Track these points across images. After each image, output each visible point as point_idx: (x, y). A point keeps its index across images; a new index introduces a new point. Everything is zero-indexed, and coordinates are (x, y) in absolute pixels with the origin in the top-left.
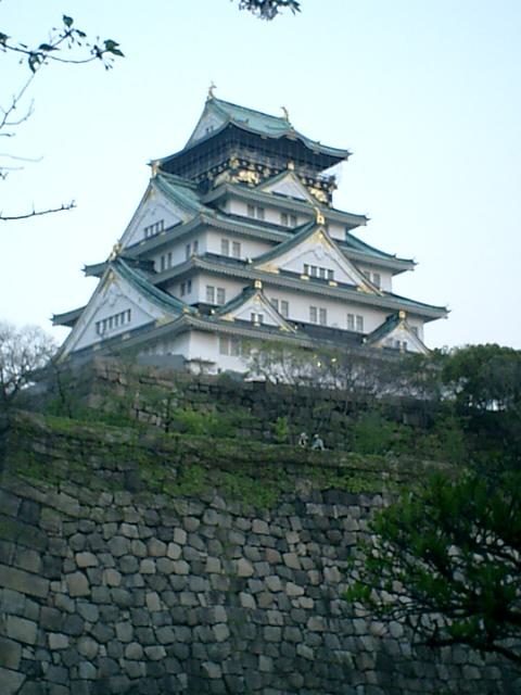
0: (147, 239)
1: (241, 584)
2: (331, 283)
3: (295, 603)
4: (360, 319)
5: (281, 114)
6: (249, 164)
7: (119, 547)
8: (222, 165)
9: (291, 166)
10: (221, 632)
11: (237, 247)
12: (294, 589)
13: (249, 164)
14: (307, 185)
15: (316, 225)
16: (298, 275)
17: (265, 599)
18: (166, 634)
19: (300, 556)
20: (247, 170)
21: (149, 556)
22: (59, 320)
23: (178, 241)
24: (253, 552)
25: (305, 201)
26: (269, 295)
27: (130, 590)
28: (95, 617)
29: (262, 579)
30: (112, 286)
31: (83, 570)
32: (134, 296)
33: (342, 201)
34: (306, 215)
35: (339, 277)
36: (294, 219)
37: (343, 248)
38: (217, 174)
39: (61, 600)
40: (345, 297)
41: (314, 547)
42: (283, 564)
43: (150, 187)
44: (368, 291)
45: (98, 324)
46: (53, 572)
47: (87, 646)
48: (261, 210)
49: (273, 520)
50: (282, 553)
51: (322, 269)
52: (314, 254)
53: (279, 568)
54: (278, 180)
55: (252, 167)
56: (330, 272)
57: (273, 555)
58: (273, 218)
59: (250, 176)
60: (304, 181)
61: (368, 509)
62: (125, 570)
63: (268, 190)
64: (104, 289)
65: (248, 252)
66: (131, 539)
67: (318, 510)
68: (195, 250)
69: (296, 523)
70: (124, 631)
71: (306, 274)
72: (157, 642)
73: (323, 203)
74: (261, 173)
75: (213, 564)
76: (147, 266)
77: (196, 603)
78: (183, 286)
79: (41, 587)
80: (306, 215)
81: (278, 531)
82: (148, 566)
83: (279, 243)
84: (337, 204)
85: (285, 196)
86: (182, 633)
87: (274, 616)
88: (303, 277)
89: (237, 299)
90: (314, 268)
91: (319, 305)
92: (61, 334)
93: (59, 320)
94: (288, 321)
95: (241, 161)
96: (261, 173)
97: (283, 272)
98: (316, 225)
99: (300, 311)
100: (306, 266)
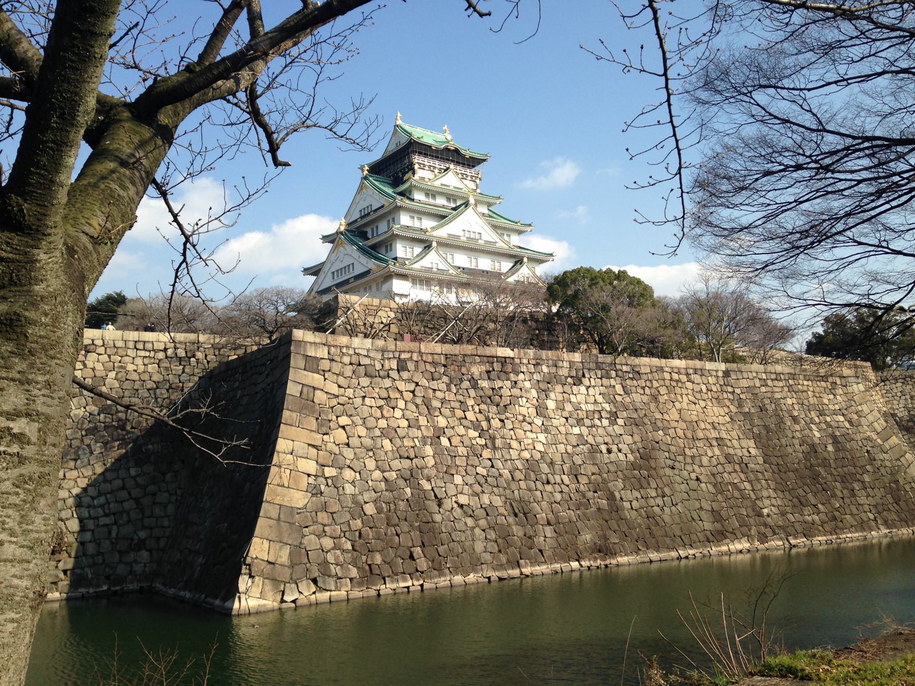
0: (362, 217)
1: (439, 433)
3: (474, 442)
7: (365, 411)
10: (431, 462)
12: (473, 433)
17: (455, 441)
18: (396, 464)
21: (383, 416)
22: (308, 271)
23: (382, 217)
24: (447, 412)
28: (352, 456)
31: (343, 427)
34: (463, 198)
36: (455, 201)
39: (331, 446)
41: (483, 407)
42: (466, 418)
45: (333, 273)
46: (324, 430)
47: (348, 474)
53: (463, 421)
55: (427, 168)
57: (459, 413)
60: (460, 176)
61: (516, 383)
62: (369, 426)
67: (485, 384)
69: (472, 392)
70: (371, 464)
75: (423, 421)
76: (363, 235)
77: (413, 445)
78: (387, 247)
79: (317, 439)
81: (461, 398)
82: (383, 423)
86: (407, 463)
87: (462, 450)
93: (308, 271)
99: (462, 260)
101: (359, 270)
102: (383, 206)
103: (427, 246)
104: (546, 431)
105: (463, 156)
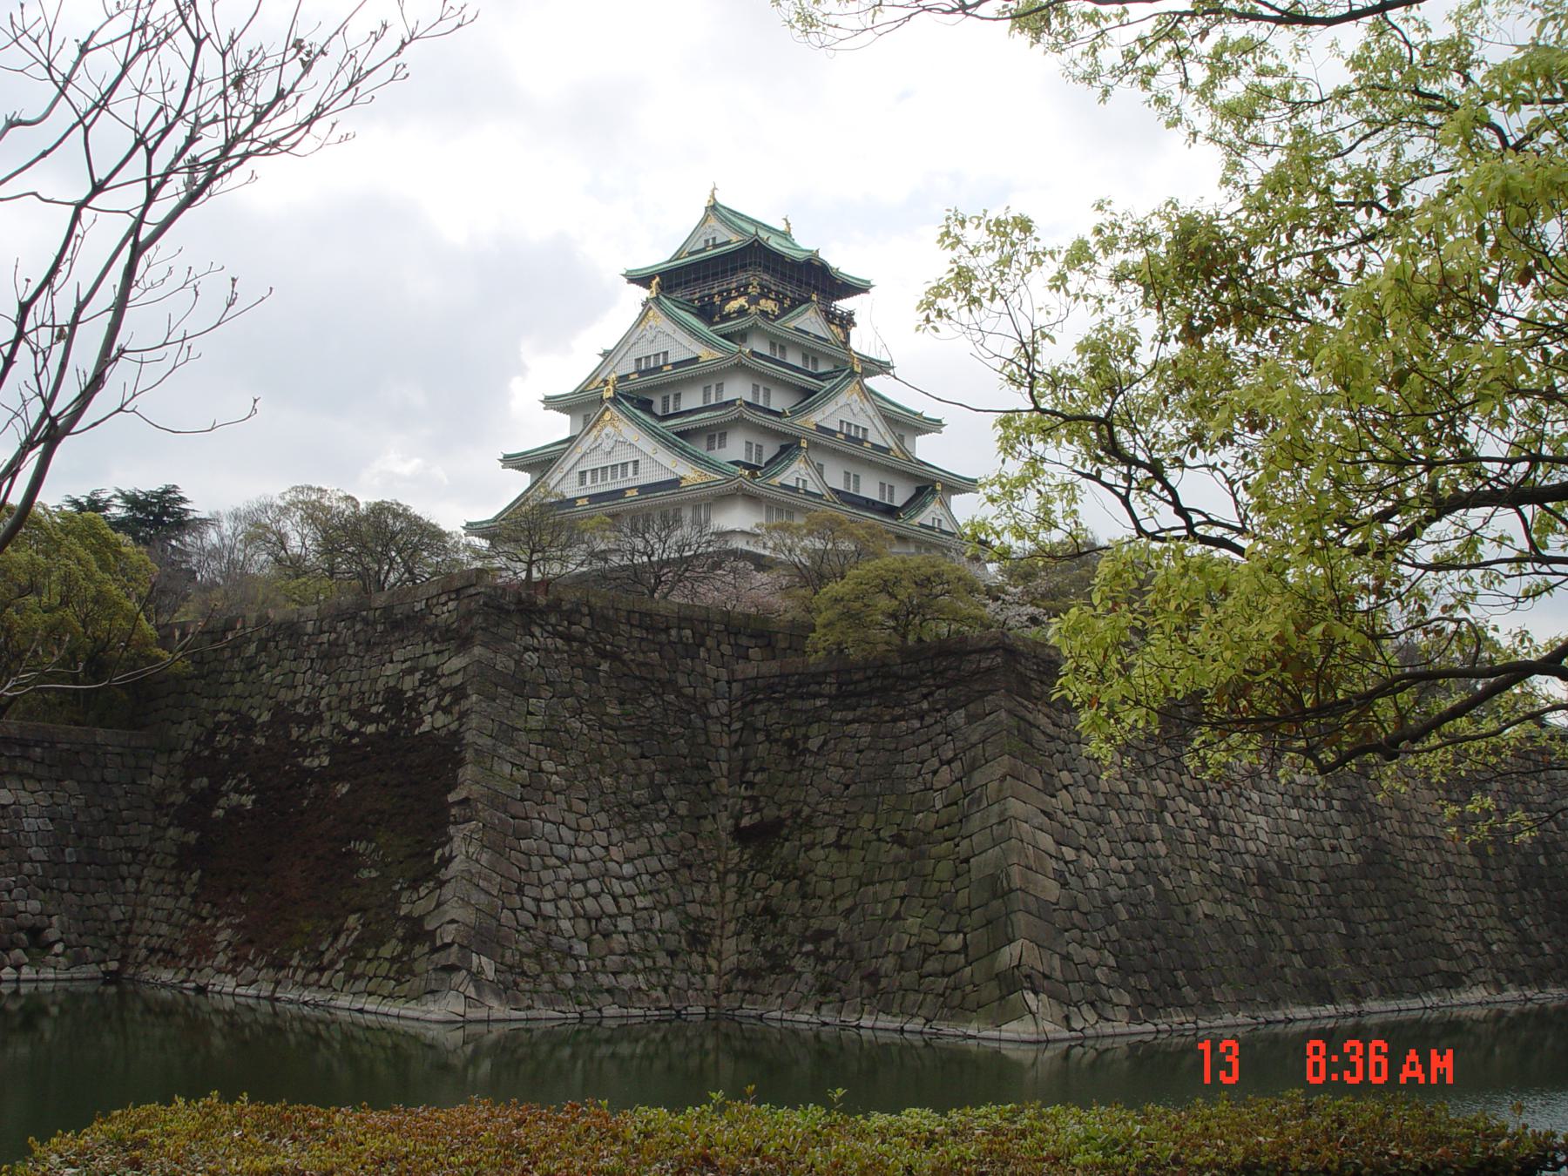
0: (641, 373)
1: (1161, 803)
5: (782, 227)
6: (770, 291)
8: (737, 289)
9: (814, 297)
11: (767, 392)
13: (770, 291)
16: (832, 433)
17: (1180, 816)
20: (768, 298)
23: (691, 381)
25: (826, 340)
30: (609, 429)
31: (1066, 787)
32: (647, 444)
33: (862, 341)
34: (829, 357)
35: (874, 437)
38: (729, 299)
45: (583, 474)
46: (1052, 790)
48: (783, 348)
51: (857, 427)
54: (802, 313)
56: (865, 430)
58: (794, 359)
59: (768, 305)
64: (595, 432)
72: (1126, 857)
75: (1142, 786)
76: (646, 406)
78: (711, 439)
80: (829, 357)
84: (854, 344)
85: (807, 333)
89: (776, 457)
90: (849, 424)
91: (853, 469)
92: (522, 480)
95: (762, 287)
97: (820, 428)
98: (853, 374)
101: (648, 476)
102: (695, 360)
104: (1265, 814)
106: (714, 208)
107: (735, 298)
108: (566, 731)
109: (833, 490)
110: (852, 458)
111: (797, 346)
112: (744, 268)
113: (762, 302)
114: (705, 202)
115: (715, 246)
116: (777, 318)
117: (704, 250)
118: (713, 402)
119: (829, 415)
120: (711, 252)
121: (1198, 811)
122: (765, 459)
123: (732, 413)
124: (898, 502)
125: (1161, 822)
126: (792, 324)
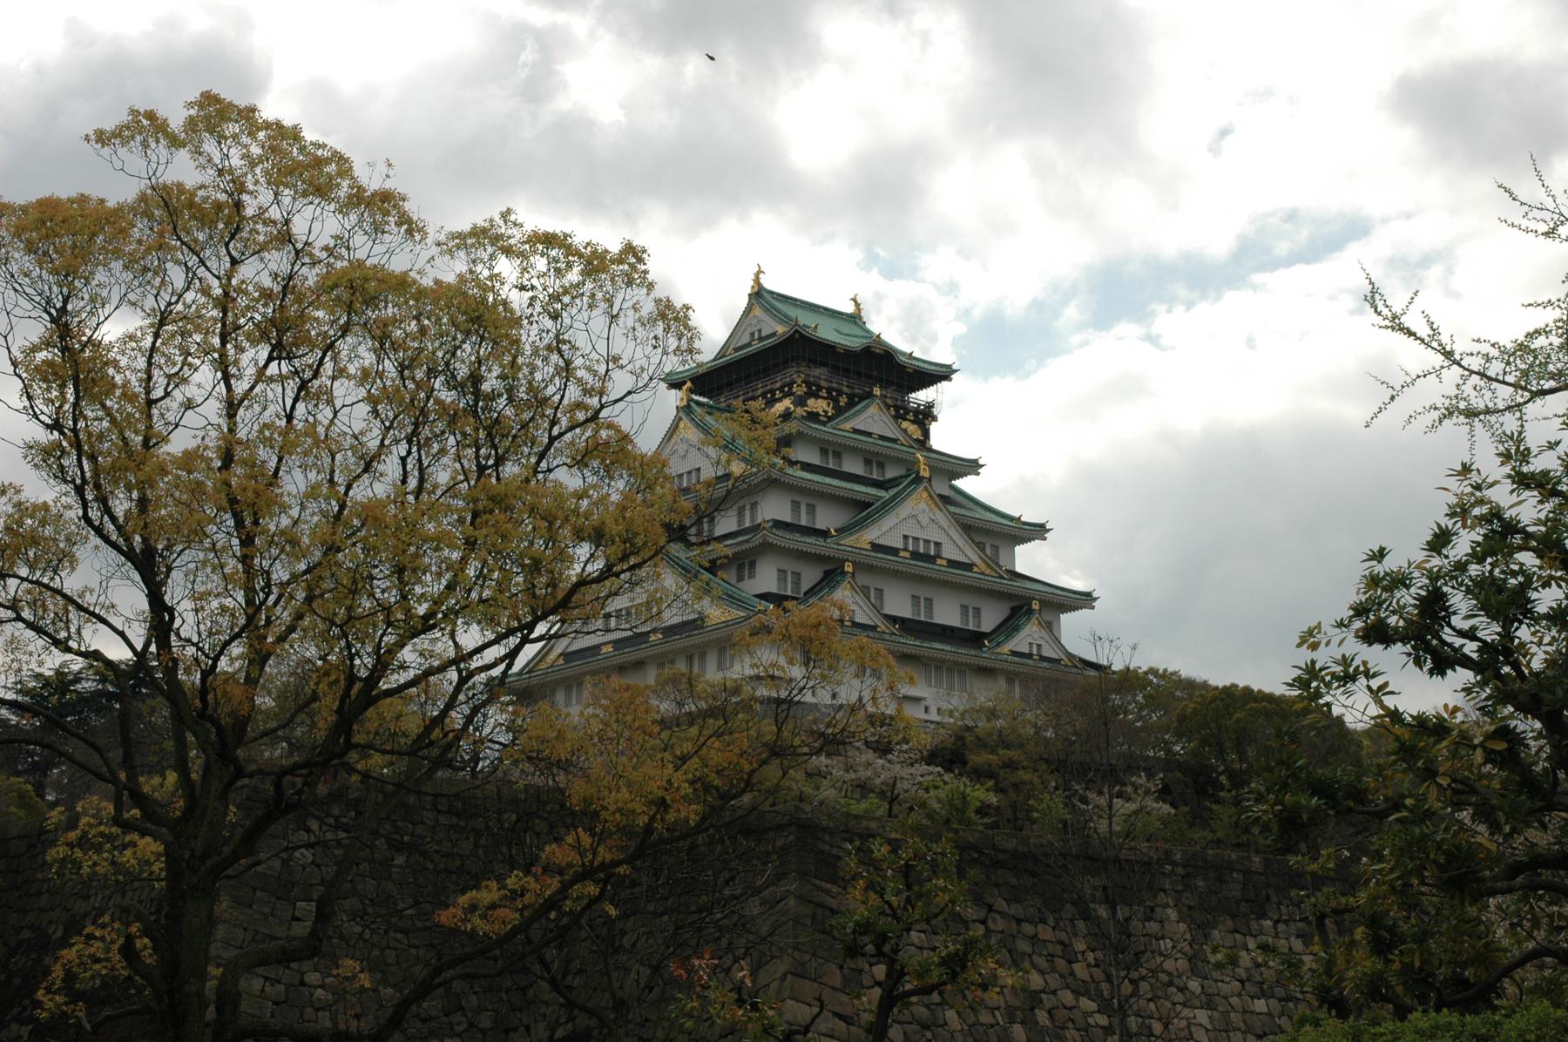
2: (939, 561)
3: (1091, 1020)
4: (977, 611)
5: (849, 308)
6: (820, 388)
8: (781, 389)
9: (877, 391)
11: (811, 510)
12: (1088, 1004)
13: (820, 388)
14: (896, 417)
15: (918, 479)
16: (894, 551)
19: (1089, 965)
20: (817, 397)
24: (1042, 962)
25: (894, 441)
26: (862, 579)
27: (927, 1006)
29: (1054, 992)
33: (942, 438)
34: (898, 461)
35: (949, 552)
36: (881, 466)
37: (952, 509)
40: (958, 580)
42: (1072, 974)
43: (677, 420)
44: (988, 571)
48: (837, 455)
49: (1057, 924)
50: (1070, 962)
51: (927, 542)
52: (910, 521)
54: (860, 411)
55: (824, 393)
56: (938, 544)
57: (1061, 964)
59: (819, 405)
61: (1152, 909)
63: (848, 426)
65: (827, 518)
66: (921, 948)
68: (753, 517)
69: (1081, 924)
71: (905, 549)
73: (917, 440)
74: (836, 401)
77: (993, 1021)
78: (741, 567)
80: (898, 461)
81: (1063, 936)
83: (871, 505)
85: (869, 434)
88: (902, 554)
90: (916, 539)
91: (923, 592)
94: (887, 617)
95: (809, 385)
96: (836, 401)
97: (876, 547)
98: (918, 479)
99: (899, 603)
100: (906, 537)
103: (832, 573)
104: (1210, 1006)
105: (901, 368)
106: (759, 295)
107: (780, 400)
108: (341, 937)
109: (893, 619)
110: (922, 579)
111: (854, 450)
112: (786, 364)
113: (811, 402)
114: (747, 288)
115: (761, 339)
116: (830, 419)
117: (749, 345)
118: (747, 524)
119: (888, 530)
120: (756, 346)
121: (1093, 1006)
122: (805, 587)
123: (757, 540)
124: (987, 626)
125: (1029, 1022)
126: (848, 426)
